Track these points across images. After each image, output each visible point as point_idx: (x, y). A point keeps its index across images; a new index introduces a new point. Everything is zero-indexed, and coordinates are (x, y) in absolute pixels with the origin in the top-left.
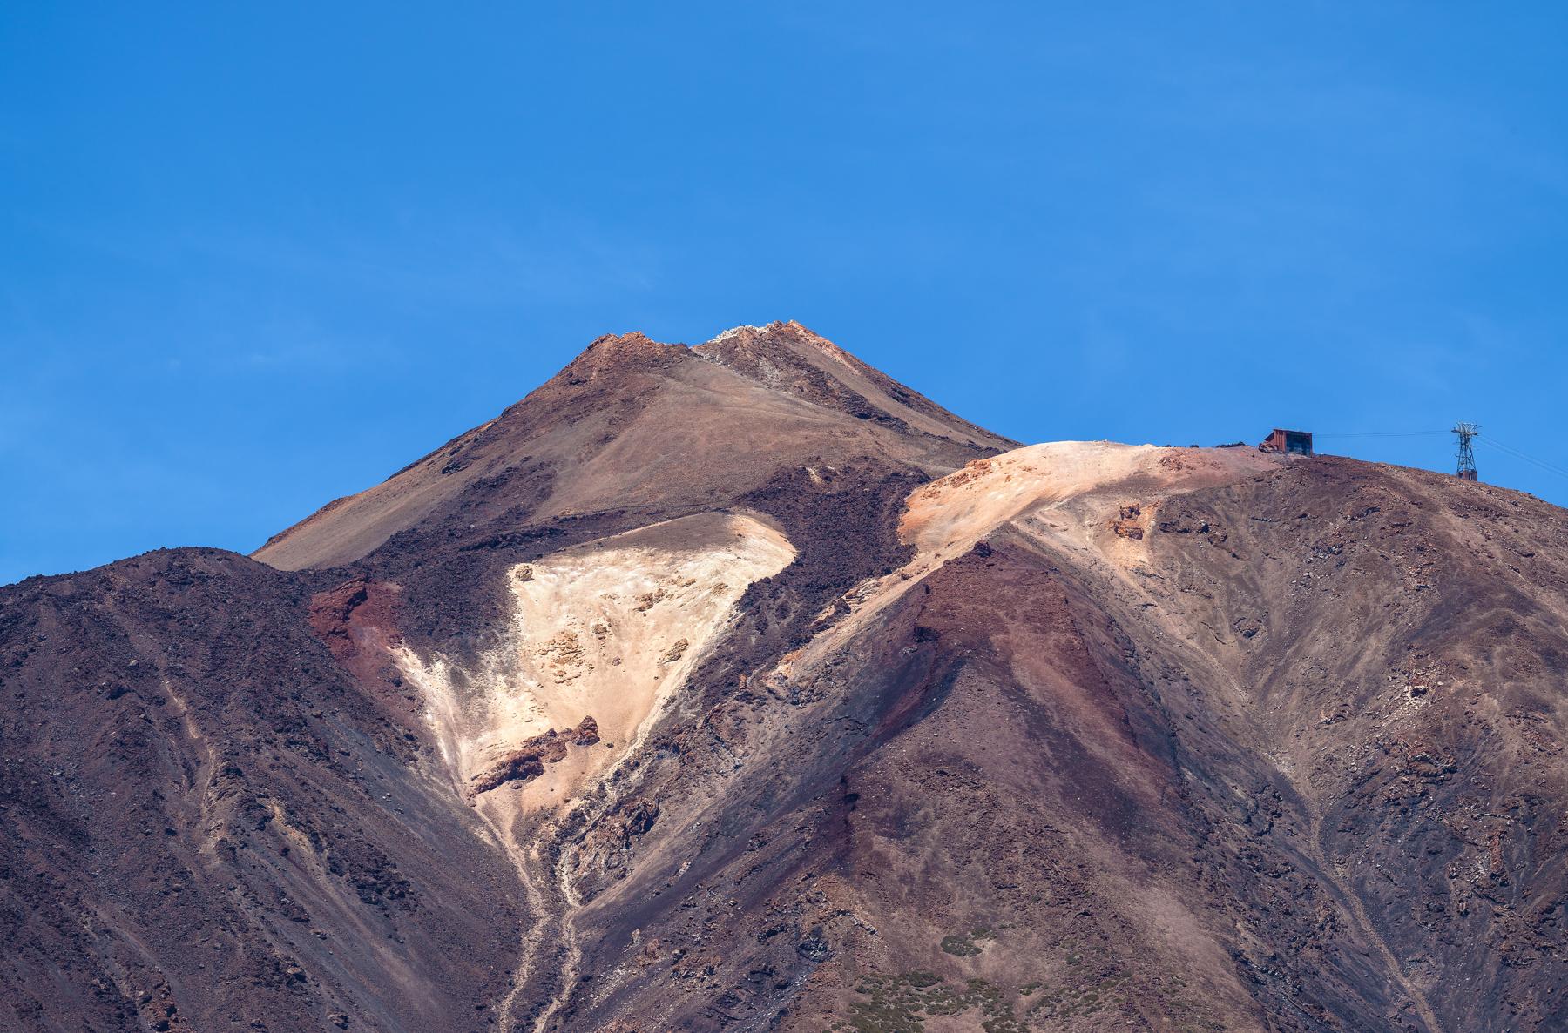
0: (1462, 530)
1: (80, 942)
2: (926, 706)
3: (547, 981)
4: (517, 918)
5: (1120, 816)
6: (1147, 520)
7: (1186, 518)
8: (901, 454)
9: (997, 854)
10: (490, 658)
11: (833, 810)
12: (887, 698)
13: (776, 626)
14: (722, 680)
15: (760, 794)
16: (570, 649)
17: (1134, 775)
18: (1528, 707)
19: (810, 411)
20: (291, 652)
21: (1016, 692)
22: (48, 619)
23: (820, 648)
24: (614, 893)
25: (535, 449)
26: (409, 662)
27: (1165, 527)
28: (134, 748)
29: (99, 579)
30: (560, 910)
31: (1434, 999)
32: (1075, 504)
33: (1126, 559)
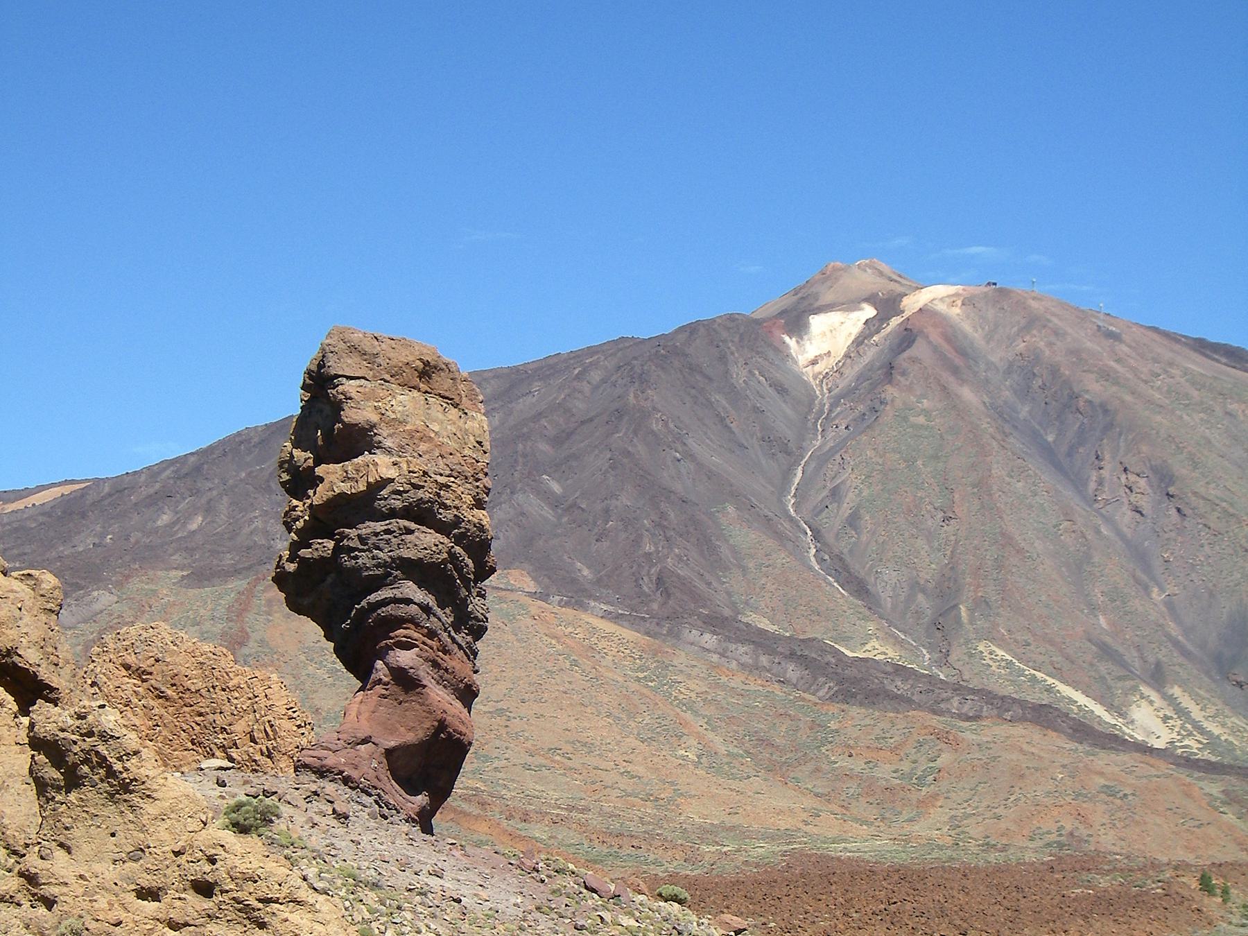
0: (1034, 304)
1: (711, 403)
2: (909, 346)
3: (821, 412)
4: (812, 397)
5: (955, 371)
6: (959, 303)
7: (968, 302)
8: (899, 289)
9: (926, 379)
10: (805, 337)
11: (889, 370)
12: (900, 345)
13: (873, 329)
14: (859, 341)
15: (870, 367)
16: (824, 334)
17: (958, 361)
18: (1050, 344)
19: (879, 280)
21: (930, 342)
22: (702, 330)
23: (883, 333)
24: (837, 391)
25: (813, 290)
26: (787, 339)
27: (963, 304)
28: (723, 359)
29: (713, 320)
30: (822, 394)
31: (1030, 412)
32: (942, 299)
33: (956, 311)
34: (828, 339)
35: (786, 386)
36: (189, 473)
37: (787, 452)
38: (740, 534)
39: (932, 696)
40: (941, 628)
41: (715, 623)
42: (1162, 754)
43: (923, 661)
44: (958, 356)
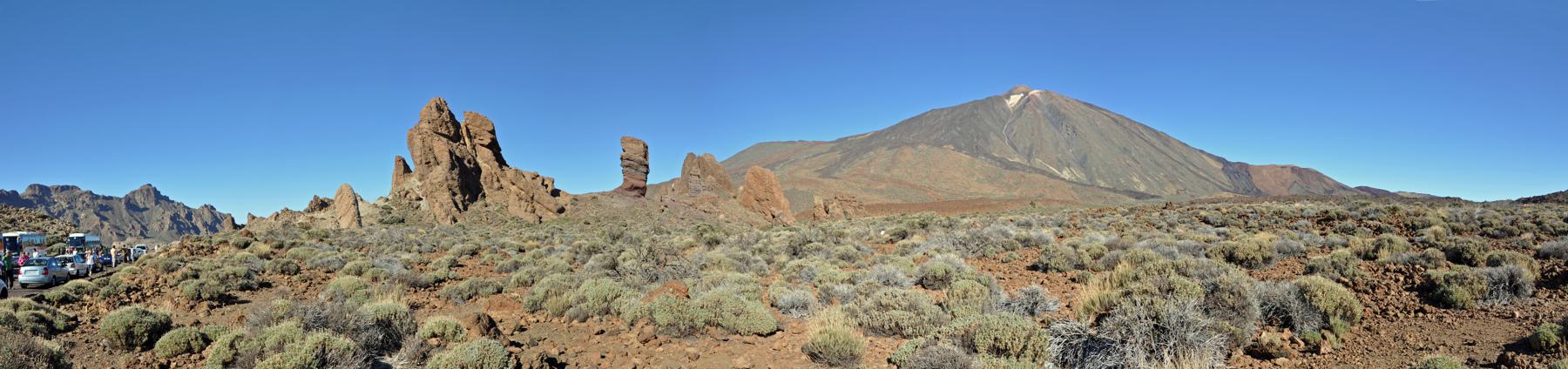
20: (1000, 99)
34: (1014, 100)
35: (1005, 109)
36: (893, 128)
37: (1004, 122)
38: (994, 138)
39: (1024, 168)
40: (1029, 156)
41: (986, 155)
42: (1070, 182)
43: (1025, 162)
44: (1038, 103)
